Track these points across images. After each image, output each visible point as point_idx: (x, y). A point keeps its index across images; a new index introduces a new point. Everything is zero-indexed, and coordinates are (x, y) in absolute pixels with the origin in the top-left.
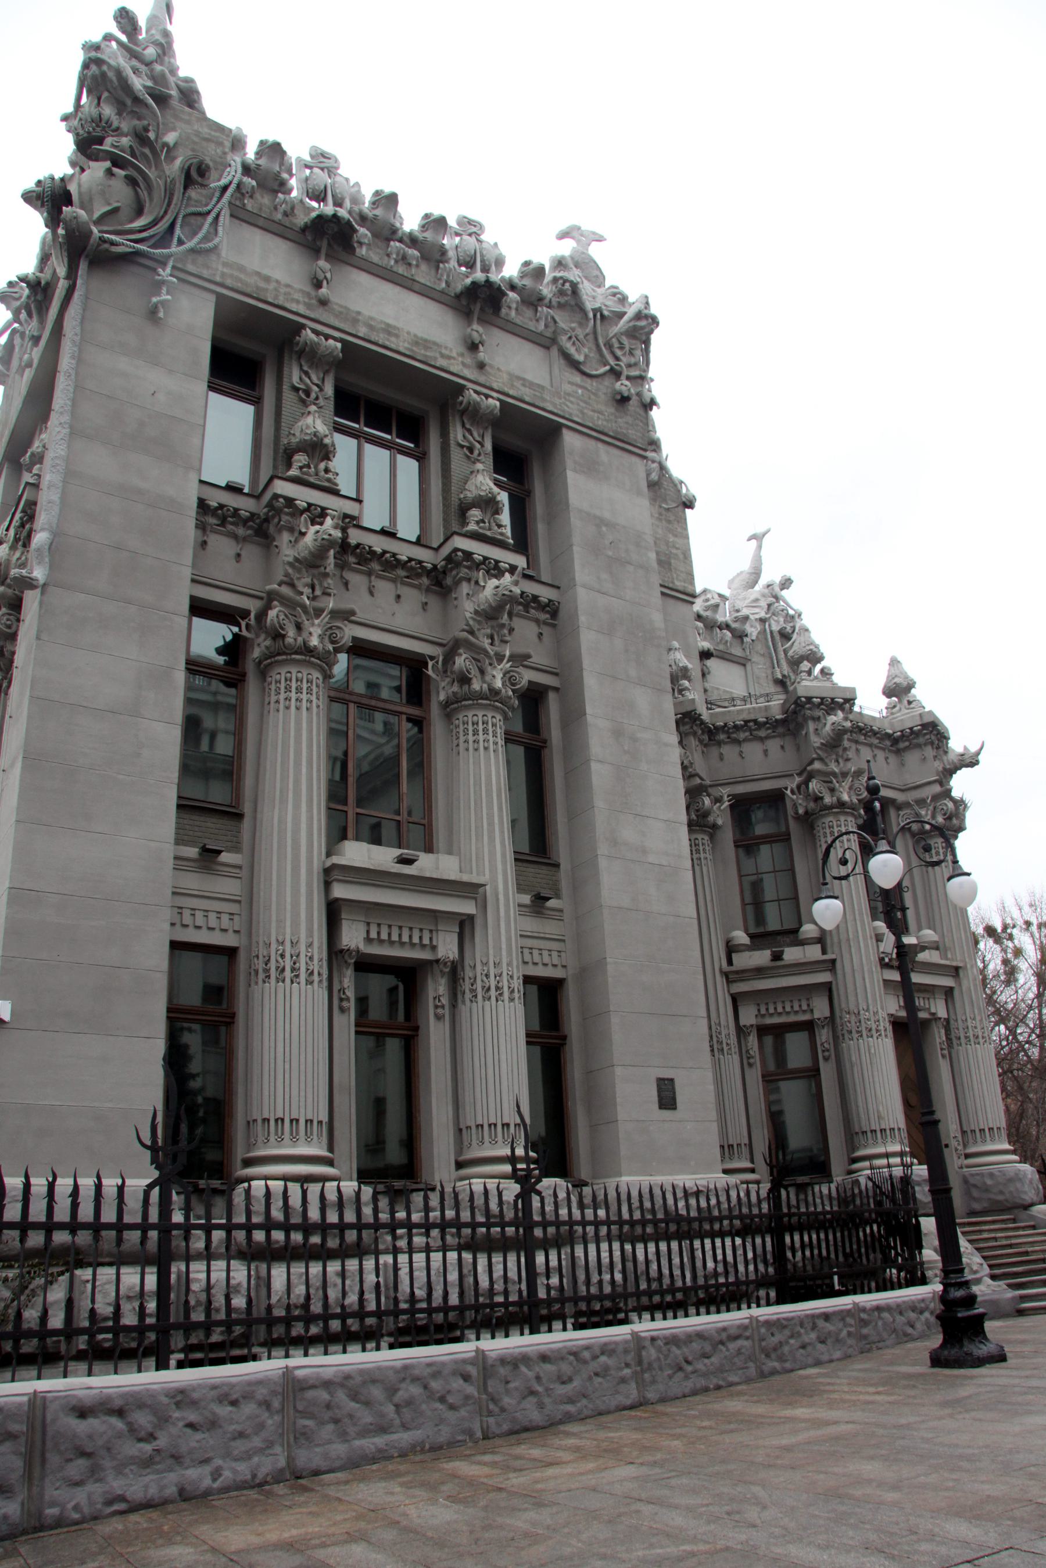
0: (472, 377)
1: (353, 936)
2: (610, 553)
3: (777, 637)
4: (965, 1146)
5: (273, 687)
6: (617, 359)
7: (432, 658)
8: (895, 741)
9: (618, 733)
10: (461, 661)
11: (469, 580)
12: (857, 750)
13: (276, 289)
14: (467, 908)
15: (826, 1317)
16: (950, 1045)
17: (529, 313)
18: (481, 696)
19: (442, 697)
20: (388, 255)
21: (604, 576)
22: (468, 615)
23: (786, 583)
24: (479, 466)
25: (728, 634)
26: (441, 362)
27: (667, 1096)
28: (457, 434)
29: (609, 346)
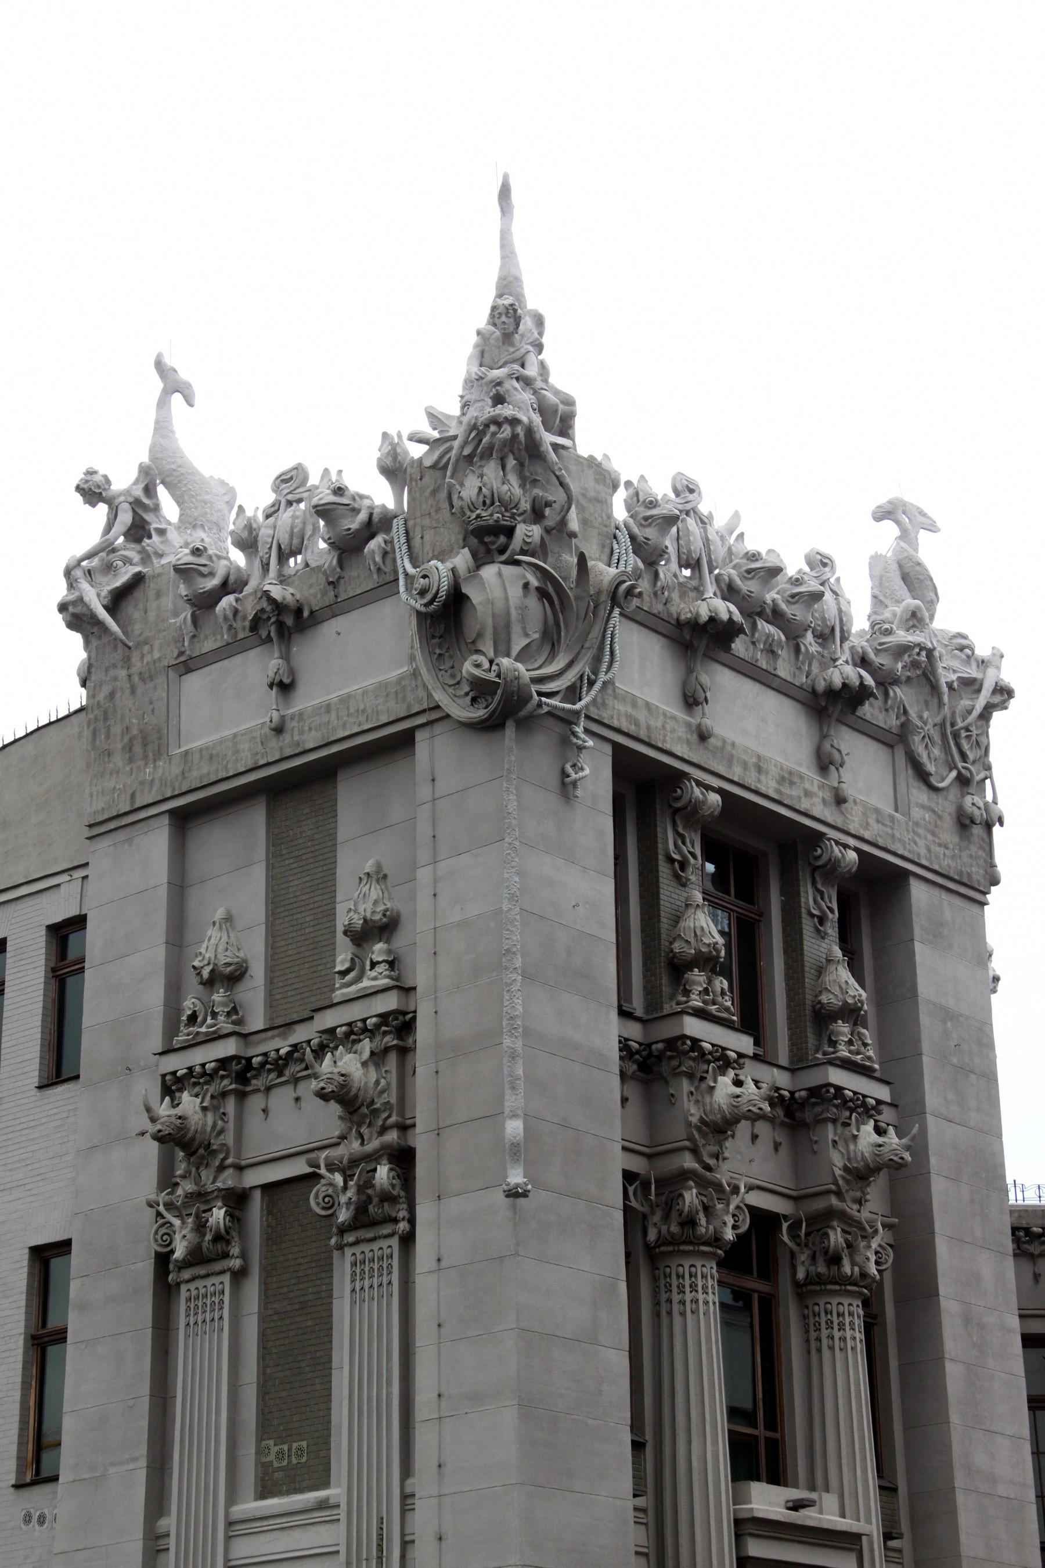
0: (830, 820)
2: (955, 1060)
5: (675, 1282)
6: (964, 757)
7: (786, 1218)
9: (967, 1320)
10: (836, 1237)
11: (834, 1121)
13: (664, 727)
18: (850, 1281)
19: (801, 1275)
20: (754, 643)
21: (951, 1096)
22: (838, 1172)
28: (808, 897)
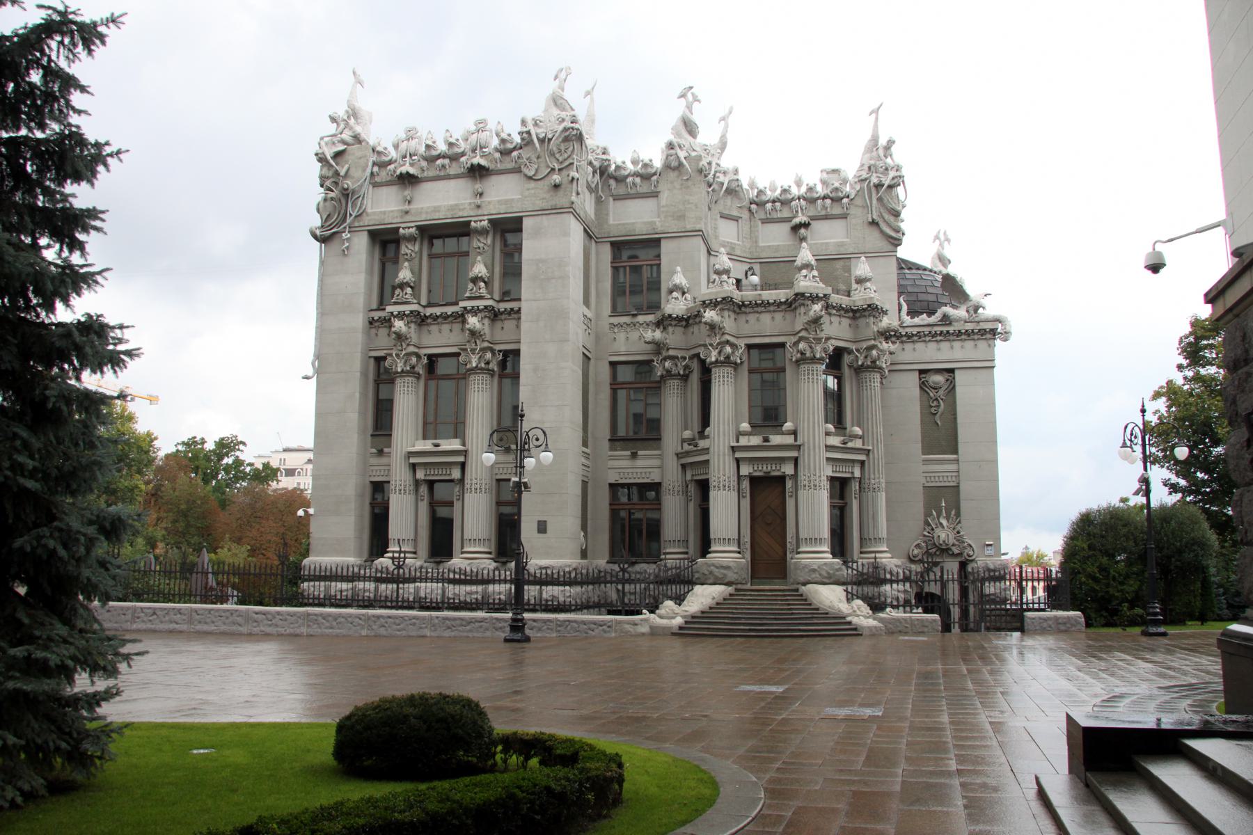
1: (420, 475)
3: (873, 190)
4: (798, 547)
8: (790, 305)
12: (758, 320)
14: (461, 459)
15: (534, 621)
16: (797, 490)
17: (507, 159)
23: (891, 143)
24: (479, 258)
25: (828, 201)
26: (461, 214)
27: (542, 527)
29: (552, 154)
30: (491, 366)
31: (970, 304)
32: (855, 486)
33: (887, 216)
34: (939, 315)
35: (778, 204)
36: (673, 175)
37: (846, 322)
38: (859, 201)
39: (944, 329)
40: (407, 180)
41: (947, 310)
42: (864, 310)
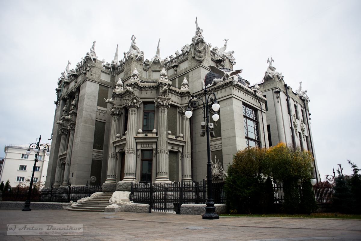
9: (77, 127)
15: (49, 204)
26: (73, 89)
30: (73, 129)
31: (225, 75)
32: (154, 152)
33: (197, 54)
34: (213, 83)
35: (170, 63)
36: (127, 62)
37: (154, 92)
38: (190, 53)
39: (213, 87)
40: (67, 84)
41: (216, 80)
42: (158, 85)
